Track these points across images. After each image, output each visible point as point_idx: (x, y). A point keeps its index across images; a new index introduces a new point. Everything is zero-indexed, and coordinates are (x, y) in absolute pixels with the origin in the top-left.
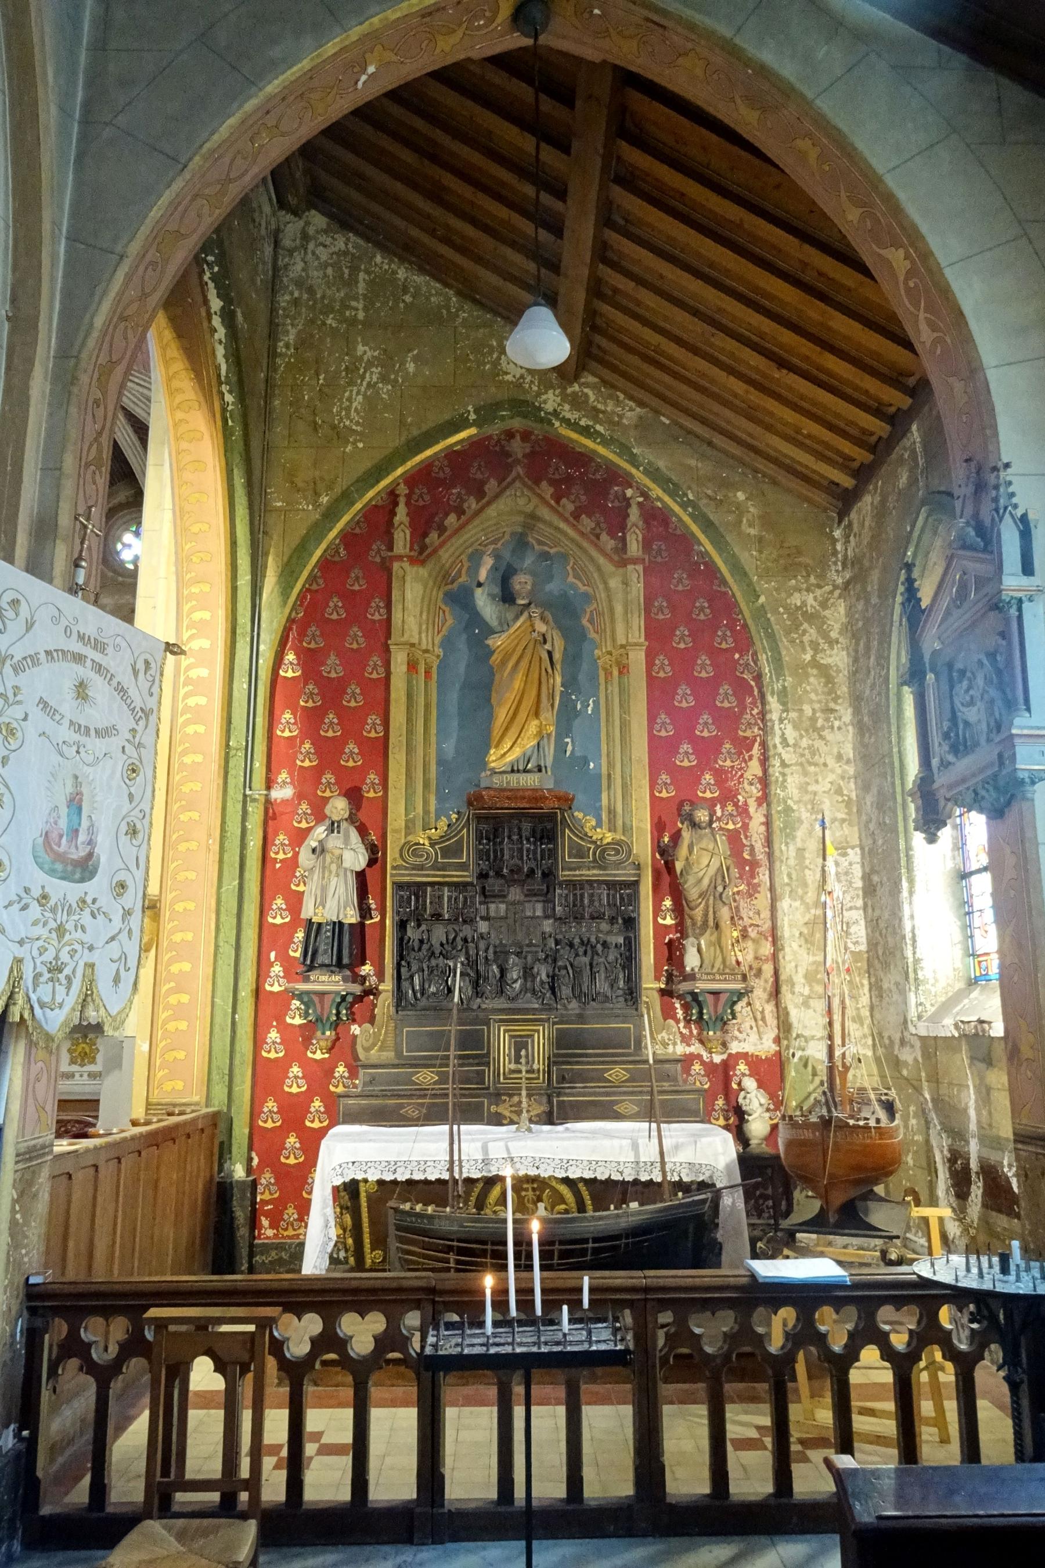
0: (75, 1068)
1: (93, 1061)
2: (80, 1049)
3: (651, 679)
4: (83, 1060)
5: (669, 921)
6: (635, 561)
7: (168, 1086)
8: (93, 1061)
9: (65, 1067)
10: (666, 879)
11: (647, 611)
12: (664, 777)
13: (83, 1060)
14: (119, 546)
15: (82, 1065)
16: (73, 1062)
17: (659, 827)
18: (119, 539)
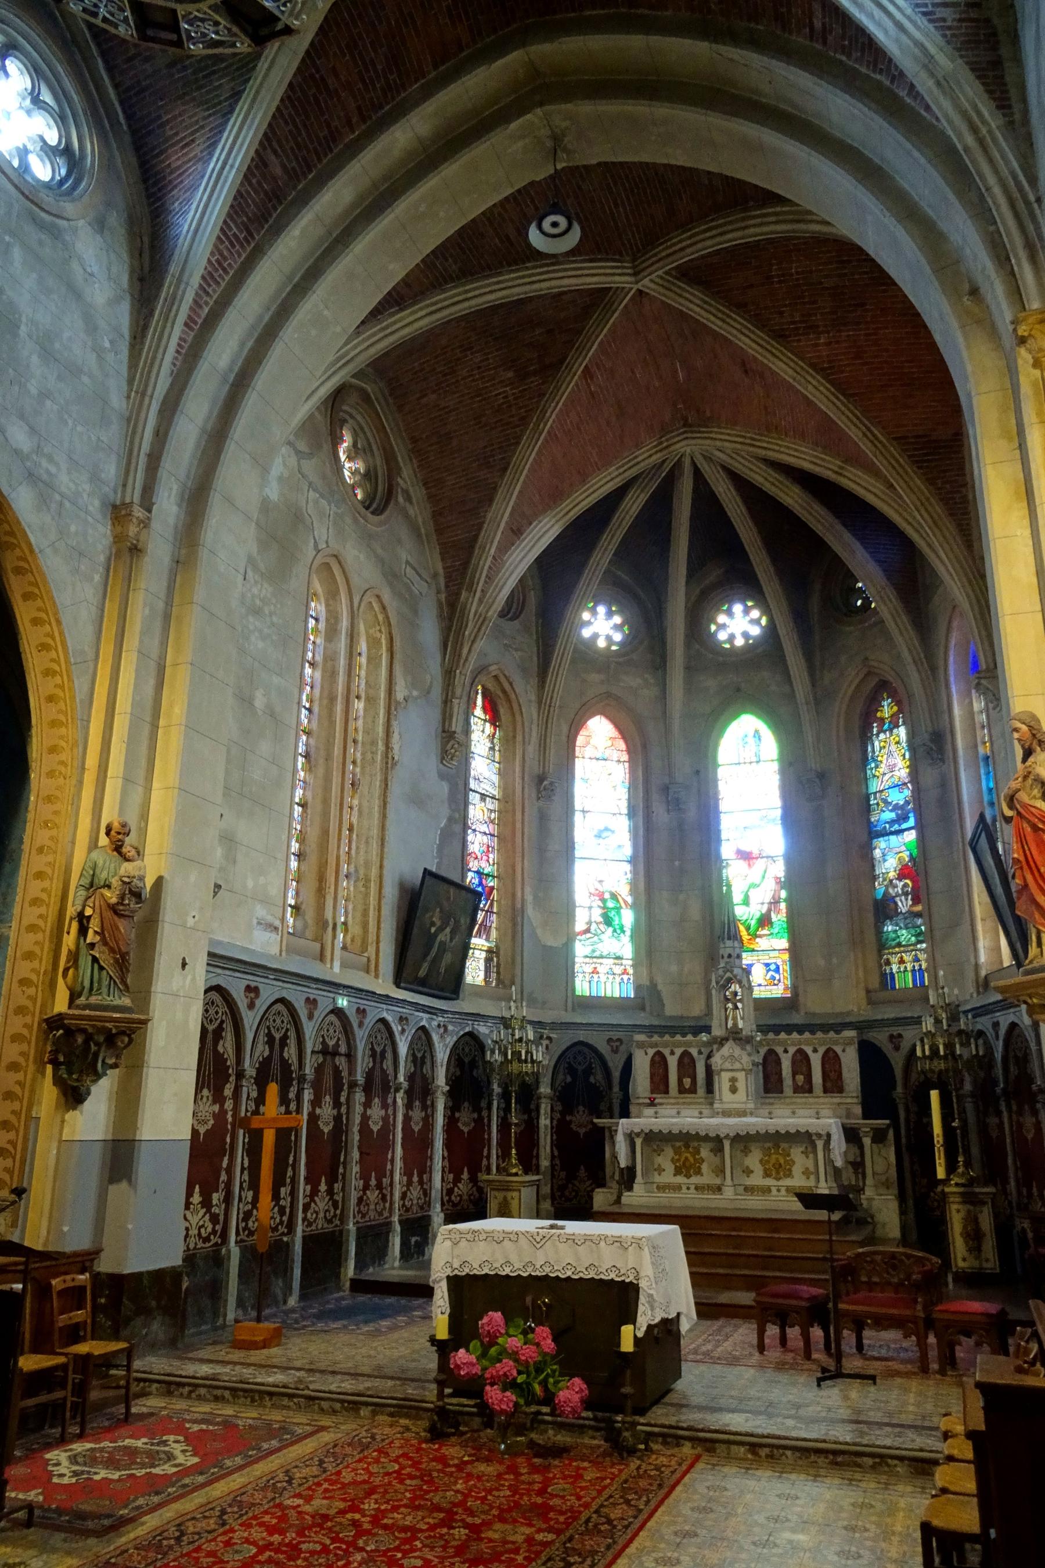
0: (770, 1182)
2: (773, 1161)
4: (778, 1173)
8: (789, 1174)
9: (757, 1179)
13: (778, 1173)
14: (713, 628)
15: (778, 1179)
18: (713, 620)
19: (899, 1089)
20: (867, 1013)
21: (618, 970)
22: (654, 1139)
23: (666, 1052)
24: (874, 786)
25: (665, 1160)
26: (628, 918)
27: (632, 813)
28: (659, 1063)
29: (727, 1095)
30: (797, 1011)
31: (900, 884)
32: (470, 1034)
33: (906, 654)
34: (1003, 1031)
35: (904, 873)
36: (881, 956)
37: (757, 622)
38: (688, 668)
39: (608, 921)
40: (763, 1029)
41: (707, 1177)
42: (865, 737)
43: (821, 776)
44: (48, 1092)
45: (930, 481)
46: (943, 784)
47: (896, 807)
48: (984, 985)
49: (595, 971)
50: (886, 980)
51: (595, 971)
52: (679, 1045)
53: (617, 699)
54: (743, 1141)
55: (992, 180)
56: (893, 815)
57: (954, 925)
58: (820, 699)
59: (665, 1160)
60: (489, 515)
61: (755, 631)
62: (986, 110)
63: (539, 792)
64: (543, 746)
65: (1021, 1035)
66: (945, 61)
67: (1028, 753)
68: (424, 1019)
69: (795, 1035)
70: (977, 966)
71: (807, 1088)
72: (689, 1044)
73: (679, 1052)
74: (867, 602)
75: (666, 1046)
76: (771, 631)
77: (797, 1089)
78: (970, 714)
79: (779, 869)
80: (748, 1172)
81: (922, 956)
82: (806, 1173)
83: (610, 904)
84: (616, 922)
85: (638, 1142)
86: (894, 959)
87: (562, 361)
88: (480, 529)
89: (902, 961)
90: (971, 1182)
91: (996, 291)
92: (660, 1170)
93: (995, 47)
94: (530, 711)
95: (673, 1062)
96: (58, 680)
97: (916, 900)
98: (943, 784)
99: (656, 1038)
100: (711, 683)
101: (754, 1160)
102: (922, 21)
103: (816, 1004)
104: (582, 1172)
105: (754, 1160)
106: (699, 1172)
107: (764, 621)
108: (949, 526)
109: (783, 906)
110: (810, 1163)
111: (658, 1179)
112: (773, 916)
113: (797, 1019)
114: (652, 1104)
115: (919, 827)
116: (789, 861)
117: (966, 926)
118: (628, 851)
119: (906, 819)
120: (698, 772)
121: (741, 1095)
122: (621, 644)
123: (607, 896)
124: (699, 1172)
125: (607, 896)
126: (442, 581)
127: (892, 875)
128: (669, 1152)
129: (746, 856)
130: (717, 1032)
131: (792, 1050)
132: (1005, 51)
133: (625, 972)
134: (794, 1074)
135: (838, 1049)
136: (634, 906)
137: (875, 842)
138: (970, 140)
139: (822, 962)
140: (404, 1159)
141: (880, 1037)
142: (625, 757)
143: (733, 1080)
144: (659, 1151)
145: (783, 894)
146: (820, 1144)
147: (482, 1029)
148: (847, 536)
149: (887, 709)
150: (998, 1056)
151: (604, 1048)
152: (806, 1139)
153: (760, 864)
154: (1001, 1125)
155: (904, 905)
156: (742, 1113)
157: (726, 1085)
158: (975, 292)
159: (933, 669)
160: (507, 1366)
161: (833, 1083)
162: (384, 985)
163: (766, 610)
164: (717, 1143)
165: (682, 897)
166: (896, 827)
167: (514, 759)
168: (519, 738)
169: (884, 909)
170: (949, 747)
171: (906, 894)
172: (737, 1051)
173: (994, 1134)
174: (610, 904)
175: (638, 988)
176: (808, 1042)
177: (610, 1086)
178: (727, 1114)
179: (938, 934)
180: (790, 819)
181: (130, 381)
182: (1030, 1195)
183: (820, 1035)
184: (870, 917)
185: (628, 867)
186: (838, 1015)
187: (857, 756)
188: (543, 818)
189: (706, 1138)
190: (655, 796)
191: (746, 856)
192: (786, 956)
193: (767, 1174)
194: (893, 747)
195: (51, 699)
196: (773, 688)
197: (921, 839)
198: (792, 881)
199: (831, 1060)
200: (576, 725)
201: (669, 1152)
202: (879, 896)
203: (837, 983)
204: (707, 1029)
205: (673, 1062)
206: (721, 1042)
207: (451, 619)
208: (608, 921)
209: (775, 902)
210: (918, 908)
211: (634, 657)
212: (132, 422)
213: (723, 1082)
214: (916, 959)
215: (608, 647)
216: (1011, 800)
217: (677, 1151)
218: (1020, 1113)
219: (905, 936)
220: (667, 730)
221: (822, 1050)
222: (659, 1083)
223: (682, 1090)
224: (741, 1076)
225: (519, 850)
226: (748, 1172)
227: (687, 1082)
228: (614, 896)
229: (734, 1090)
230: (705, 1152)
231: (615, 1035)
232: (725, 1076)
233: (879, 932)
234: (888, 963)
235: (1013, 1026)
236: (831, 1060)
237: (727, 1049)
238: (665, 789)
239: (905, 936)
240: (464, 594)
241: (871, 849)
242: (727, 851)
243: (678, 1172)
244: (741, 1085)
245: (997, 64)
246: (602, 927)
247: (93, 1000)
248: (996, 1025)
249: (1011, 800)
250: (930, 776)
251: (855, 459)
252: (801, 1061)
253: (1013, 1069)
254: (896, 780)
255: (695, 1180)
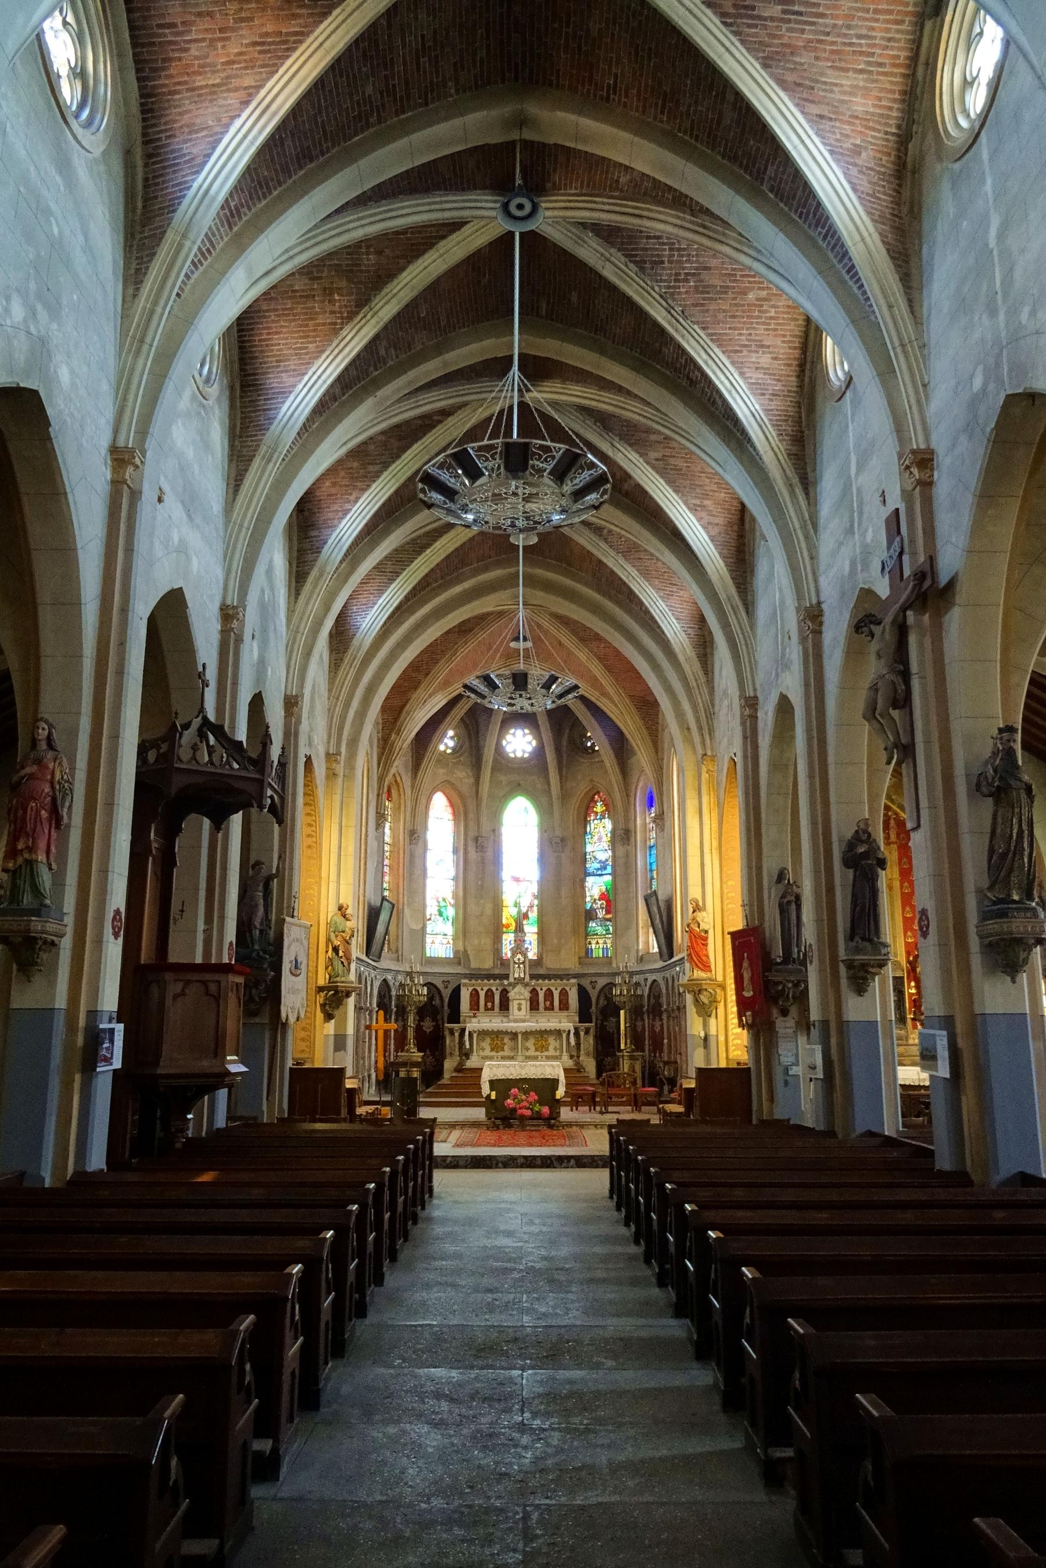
0: (538, 1053)
1: (547, 1050)
3: (902, 893)
5: (913, 991)
6: (893, 843)
7: (736, 1053)
8: (547, 1050)
10: (912, 974)
11: (900, 864)
12: (909, 934)
16: (536, 1050)
17: (908, 953)
19: (594, 1008)
20: (579, 970)
21: (445, 942)
22: (483, 1034)
23: (479, 989)
24: (589, 848)
25: (486, 1044)
26: (451, 912)
27: (455, 851)
28: (475, 995)
29: (516, 1012)
30: (541, 966)
31: (600, 903)
32: (385, 980)
33: (613, 779)
34: (649, 983)
35: (603, 897)
36: (586, 939)
37: (530, 743)
38: (493, 769)
39: (440, 914)
40: (533, 977)
41: (507, 1052)
42: (586, 822)
43: (563, 840)
44: (320, 1016)
45: (643, 719)
46: (627, 855)
47: (600, 862)
48: (641, 960)
49: (433, 942)
50: (588, 952)
51: (433, 942)
52: (486, 985)
53: (452, 784)
54: (527, 1034)
55: (700, 700)
56: (598, 866)
57: (627, 928)
58: (565, 796)
59: (486, 1044)
60: (415, 696)
61: (529, 749)
62: (701, 673)
63: (411, 840)
64: (414, 815)
65: (658, 985)
66: (690, 652)
67: (694, 911)
68: (373, 973)
69: (547, 981)
70: (638, 950)
71: (551, 1008)
72: (492, 985)
73: (486, 989)
74: (593, 745)
75: (479, 985)
76: (539, 752)
77: (546, 1009)
78: (645, 824)
79: (534, 889)
80: (527, 1049)
81: (609, 941)
82: (555, 1049)
83: (442, 904)
84: (444, 915)
85: (475, 1035)
86: (594, 942)
87: (470, 631)
88: (407, 702)
89: (597, 943)
90: (633, 1051)
91: (697, 739)
92: (483, 1049)
93: (705, 648)
94: (408, 791)
95: (482, 994)
96: (314, 839)
97: (608, 912)
98: (627, 855)
99: (473, 981)
100: (503, 778)
101: (530, 1044)
102: (683, 634)
103: (552, 963)
104: (428, 1052)
105: (530, 1044)
106: (503, 1050)
107: (534, 743)
108: (648, 739)
109: (535, 909)
110: (557, 1044)
111: (481, 1053)
112: (530, 914)
113: (542, 971)
114: (475, 1016)
115: (614, 874)
116: (541, 883)
117: (634, 930)
118: (452, 873)
119: (605, 868)
120: (494, 831)
121: (523, 1012)
122: (454, 749)
123: (441, 900)
124: (503, 1050)
125: (441, 900)
126: (381, 727)
127: (597, 897)
128: (488, 1040)
129: (517, 880)
130: (511, 980)
131: (545, 989)
132: (709, 651)
133: (448, 943)
134: (545, 1000)
135: (568, 989)
136: (456, 906)
137: (588, 879)
138: (694, 684)
139: (555, 941)
140: (395, 1044)
141: (586, 983)
142: (451, 817)
143: (520, 1004)
144: (483, 1040)
145: (536, 902)
146: (564, 1035)
147: (389, 977)
148: (593, 721)
149: (599, 808)
150: (646, 994)
151: (441, 986)
152: (558, 1033)
153: (523, 884)
154: (644, 1025)
155: (601, 914)
156: (524, 1021)
157: (516, 1007)
158: (688, 729)
159: (628, 796)
160: (525, 1104)
161: (564, 1006)
162: (364, 958)
163: (538, 736)
164: (514, 1036)
165: (482, 901)
166: (599, 872)
167: (399, 821)
168: (402, 809)
169: (590, 915)
170: (632, 839)
171: (602, 908)
172: (523, 990)
173: (639, 1029)
174: (442, 904)
175: (456, 952)
176: (553, 985)
177: (443, 1007)
178: (516, 1021)
179: (619, 932)
180: (542, 859)
181: (330, 691)
182: (655, 1056)
183: (558, 981)
184: (583, 919)
185: (452, 883)
186: (563, 969)
187: (581, 831)
188: (412, 855)
189: (506, 1033)
190: (471, 843)
191: (517, 880)
192: (536, 936)
193: (536, 1050)
194: (601, 829)
195: (309, 847)
196: (539, 786)
197: (614, 880)
198: (541, 895)
199: (564, 994)
200: (429, 799)
201: (488, 1040)
202: (588, 906)
203: (563, 952)
204: (507, 977)
205: (482, 994)
206: (514, 985)
207: (384, 748)
208: (440, 914)
209: (531, 906)
210: (609, 916)
211: (462, 759)
212: (330, 711)
213: (513, 1006)
214: (605, 943)
215: (445, 751)
216: (688, 926)
217: (492, 1039)
218: (654, 1020)
219: (600, 930)
220: (478, 806)
221: (559, 989)
222: (475, 1005)
223: (486, 1009)
224: (523, 1002)
225: (401, 875)
226: (527, 1049)
227: (489, 1005)
228: (444, 900)
229: (520, 1009)
230: (506, 1040)
231: (445, 979)
232: (516, 1002)
233: (586, 927)
234: (590, 943)
235: (655, 981)
236: (564, 994)
237: (517, 989)
238: (476, 839)
239: (600, 930)
240: (393, 736)
241: (583, 881)
242: (506, 874)
243: (492, 1050)
244: (523, 1007)
245: (705, 655)
246: (438, 917)
247: (343, 979)
248: (646, 980)
249: (688, 926)
250: (621, 850)
251: (605, 694)
252: (549, 994)
253: (652, 1001)
254: (601, 847)
255: (501, 1053)
